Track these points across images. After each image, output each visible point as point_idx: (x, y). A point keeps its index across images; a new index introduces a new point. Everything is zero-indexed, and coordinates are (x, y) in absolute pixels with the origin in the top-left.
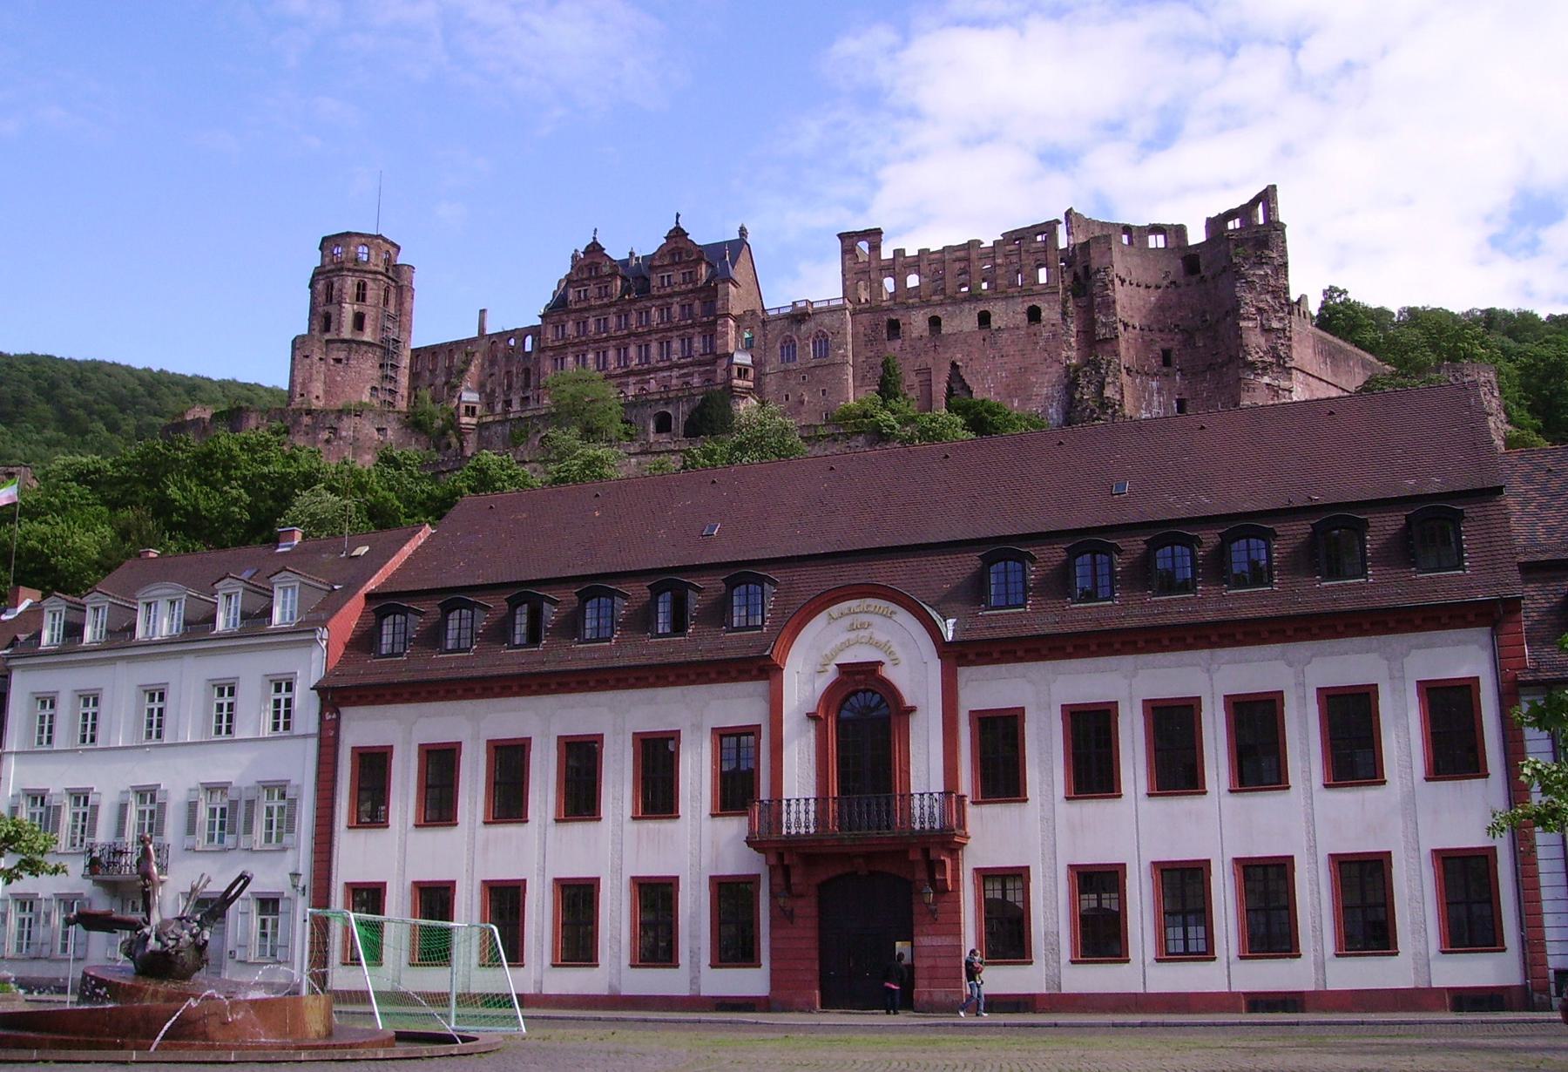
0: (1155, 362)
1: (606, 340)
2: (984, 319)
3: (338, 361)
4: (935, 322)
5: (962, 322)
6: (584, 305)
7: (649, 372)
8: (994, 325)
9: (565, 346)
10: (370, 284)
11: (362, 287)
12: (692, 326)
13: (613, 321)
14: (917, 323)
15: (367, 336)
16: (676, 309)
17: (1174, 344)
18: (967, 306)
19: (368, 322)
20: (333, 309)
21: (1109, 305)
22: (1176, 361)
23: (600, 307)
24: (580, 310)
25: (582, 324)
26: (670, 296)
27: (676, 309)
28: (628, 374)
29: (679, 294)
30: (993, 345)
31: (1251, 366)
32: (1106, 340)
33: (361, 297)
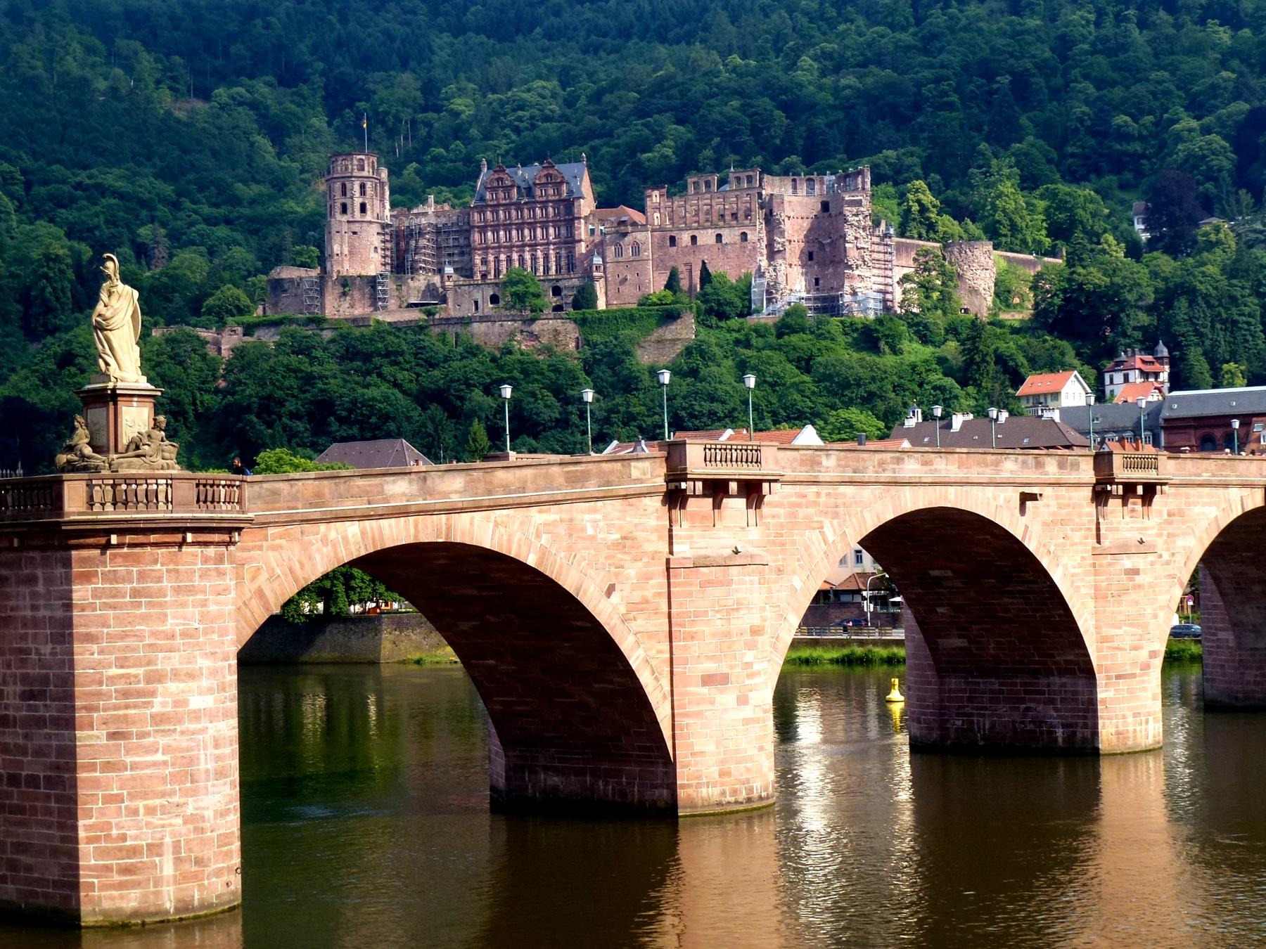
2: (719, 237)
3: (355, 233)
4: (694, 238)
9: (486, 226)
10: (369, 185)
11: (363, 187)
14: (685, 238)
15: (369, 217)
16: (551, 210)
17: (815, 249)
19: (368, 207)
20: (348, 201)
21: (782, 234)
27: (551, 210)
30: (723, 252)
31: (850, 267)
32: (779, 251)
33: (363, 193)
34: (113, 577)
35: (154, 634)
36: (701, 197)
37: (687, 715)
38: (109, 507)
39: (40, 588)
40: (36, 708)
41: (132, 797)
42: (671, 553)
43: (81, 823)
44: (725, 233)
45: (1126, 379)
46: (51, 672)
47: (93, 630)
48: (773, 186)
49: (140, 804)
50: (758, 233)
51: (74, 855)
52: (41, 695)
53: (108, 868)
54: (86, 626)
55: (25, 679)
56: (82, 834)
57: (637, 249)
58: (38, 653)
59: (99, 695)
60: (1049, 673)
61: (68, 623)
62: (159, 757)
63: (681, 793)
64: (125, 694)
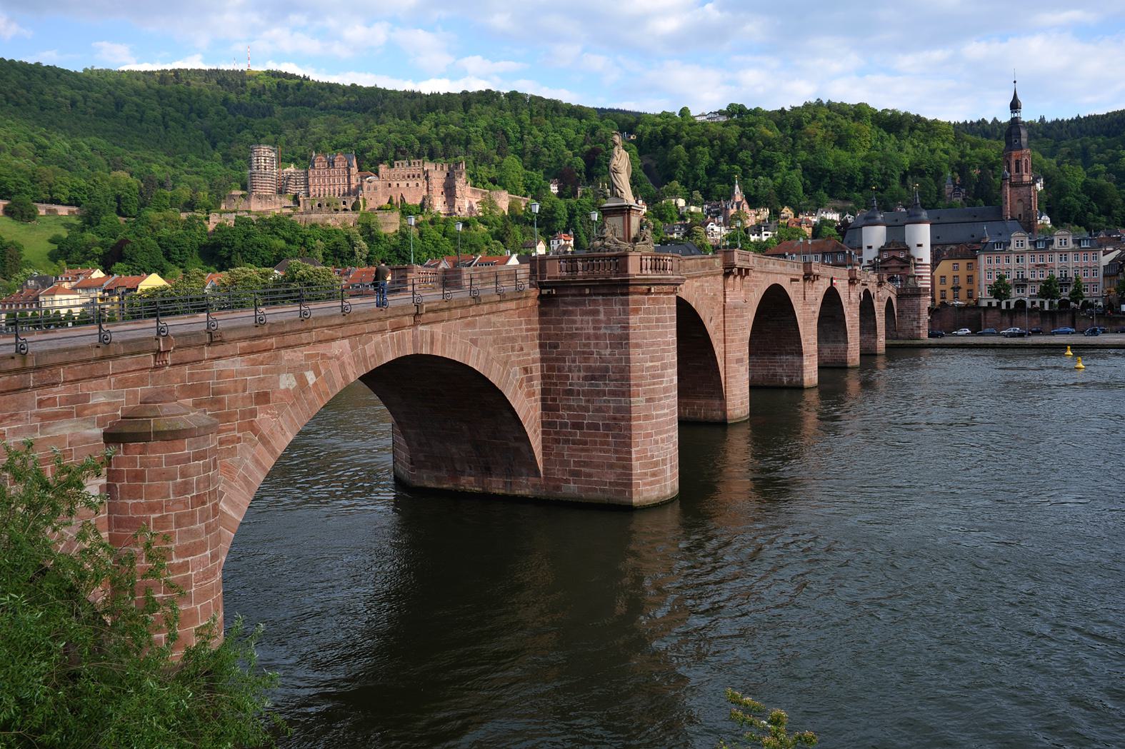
14: (394, 184)
21: (432, 184)
25: (319, 173)
34: (648, 311)
35: (664, 342)
36: (402, 168)
37: (731, 377)
38: (650, 272)
39: (602, 317)
40: (597, 385)
41: (657, 434)
42: (725, 302)
43: (633, 450)
44: (410, 183)
45: (558, 242)
46: (610, 365)
47: (639, 341)
48: (429, 166)
49: (659, 437)
50: (422, 183)
51: (629, 468)
52: (603, 378)
53: (646, 474)
54: (636, 339)
55: (588, 369)
56: (634, 456)
57: (375, 188)
58: (599, 353)
59: (641, 377)
60: (781, 354)
61: (627, 337)
62: (666, 411)
63: (728, 413)
64: (653, 377)
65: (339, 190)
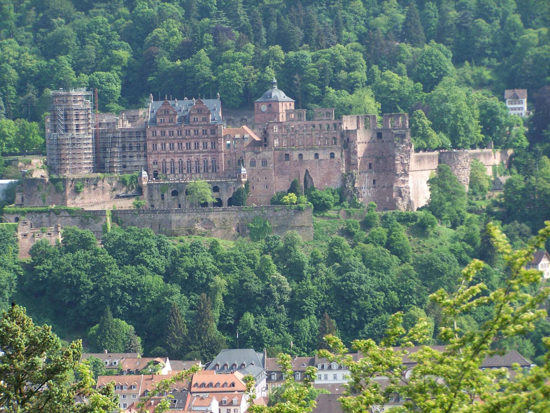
0: (367, 168)
1: (174, 139)
2: (317, 156)
4: (301, 155)
5: (309, 156)
6: (164, 125)
7: (191, 153)
8: (320, 158)
9: (157, 140)
12: (207, 138)
13: (176, 132)
14: (295, 155)
16: (200, 131)
17: (373, 161)
18: (311, 151)
21: (355, 153)
22: (372, 166)
23: (170, 126)
24: (163, 127)
25: (163, 133)
26: (198, 125)
28: (183, 153)
29: (202, 125)
30: (319, 164)
31: (398, 175)
57: (265, 163)
65: (198, 162)
